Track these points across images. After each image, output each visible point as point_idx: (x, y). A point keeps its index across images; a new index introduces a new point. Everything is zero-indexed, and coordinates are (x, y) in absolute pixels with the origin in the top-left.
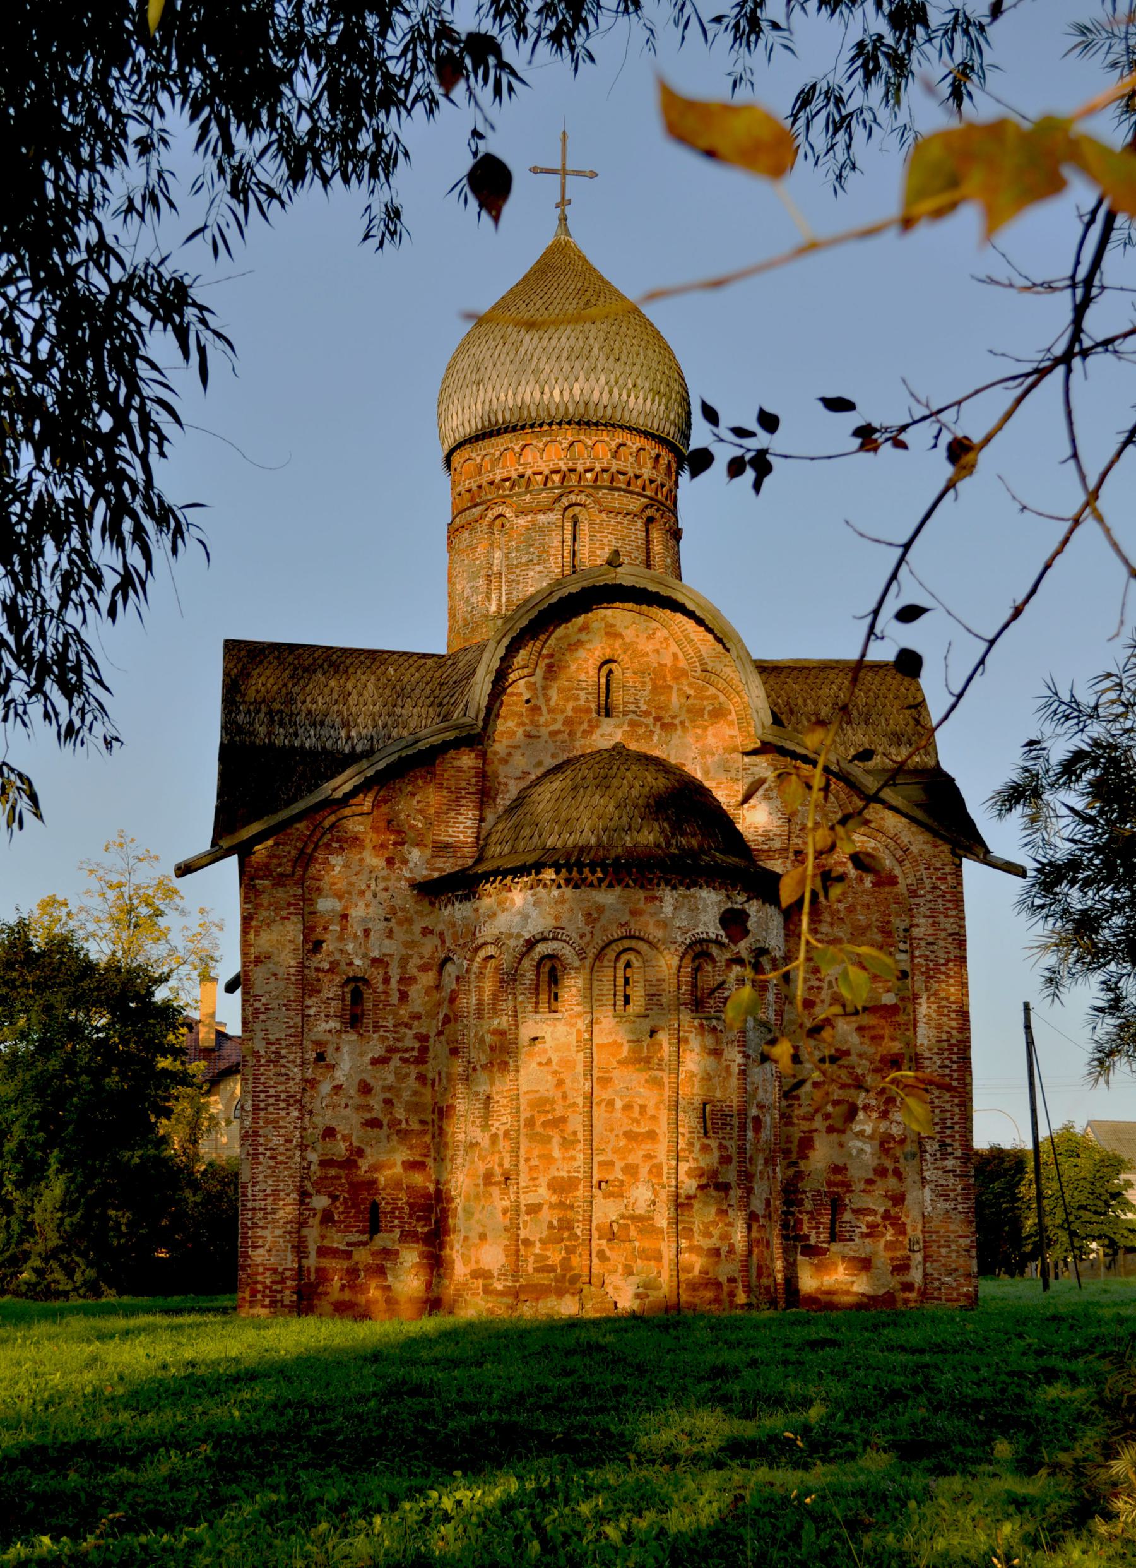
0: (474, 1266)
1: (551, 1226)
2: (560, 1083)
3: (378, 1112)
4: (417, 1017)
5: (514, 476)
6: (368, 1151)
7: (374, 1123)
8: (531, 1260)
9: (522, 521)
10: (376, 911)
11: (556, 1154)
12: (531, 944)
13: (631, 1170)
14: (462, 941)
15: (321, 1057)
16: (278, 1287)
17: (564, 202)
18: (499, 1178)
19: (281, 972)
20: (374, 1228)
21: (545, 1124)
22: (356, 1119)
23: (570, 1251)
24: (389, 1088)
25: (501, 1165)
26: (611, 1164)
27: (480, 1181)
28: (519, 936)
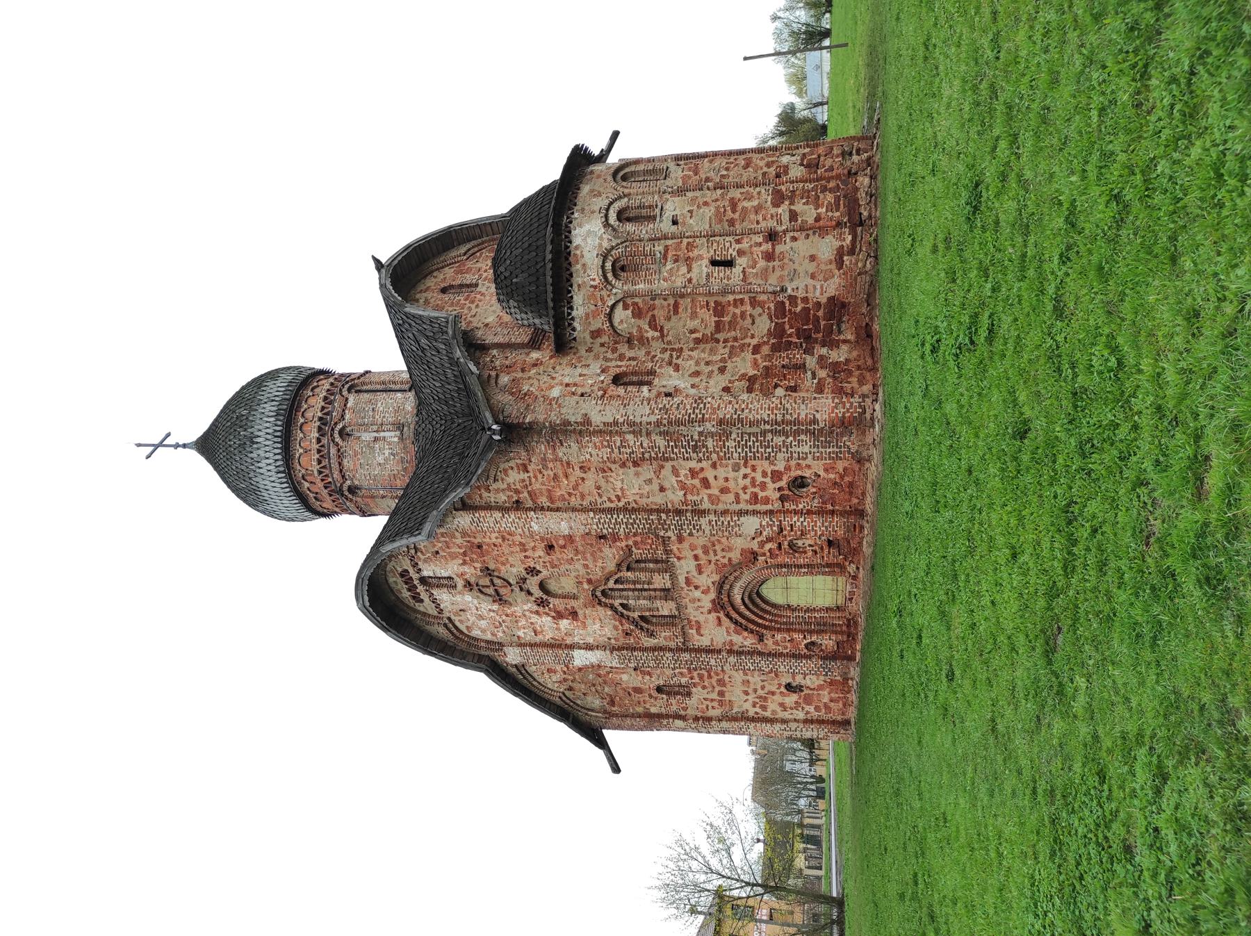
0: (833, 266)
1: (806, 203)
2: (706, 204)
3: (715, 368)
4: (648, 353)
5: (318, 423)
6: (743, 371)
7: (722, 370)
8: (830, 214)
9: (347, 417)
10: (568, 370)
11: (755, 203)
12: (607, 224)
13: (768, 165)
14: (600, 303)
15: (668, 395)
16: (848, 405)
17: (177, 446)
18: (767, 247)
19: (598, 408)
20: (802, 367)
21: (734, 211)
22: (720, 377)
23: (824, 189)
24: (697, 363)
25: (760, 245)
26: (764, 174)
27: (771, 264)
28: (601, 238)
